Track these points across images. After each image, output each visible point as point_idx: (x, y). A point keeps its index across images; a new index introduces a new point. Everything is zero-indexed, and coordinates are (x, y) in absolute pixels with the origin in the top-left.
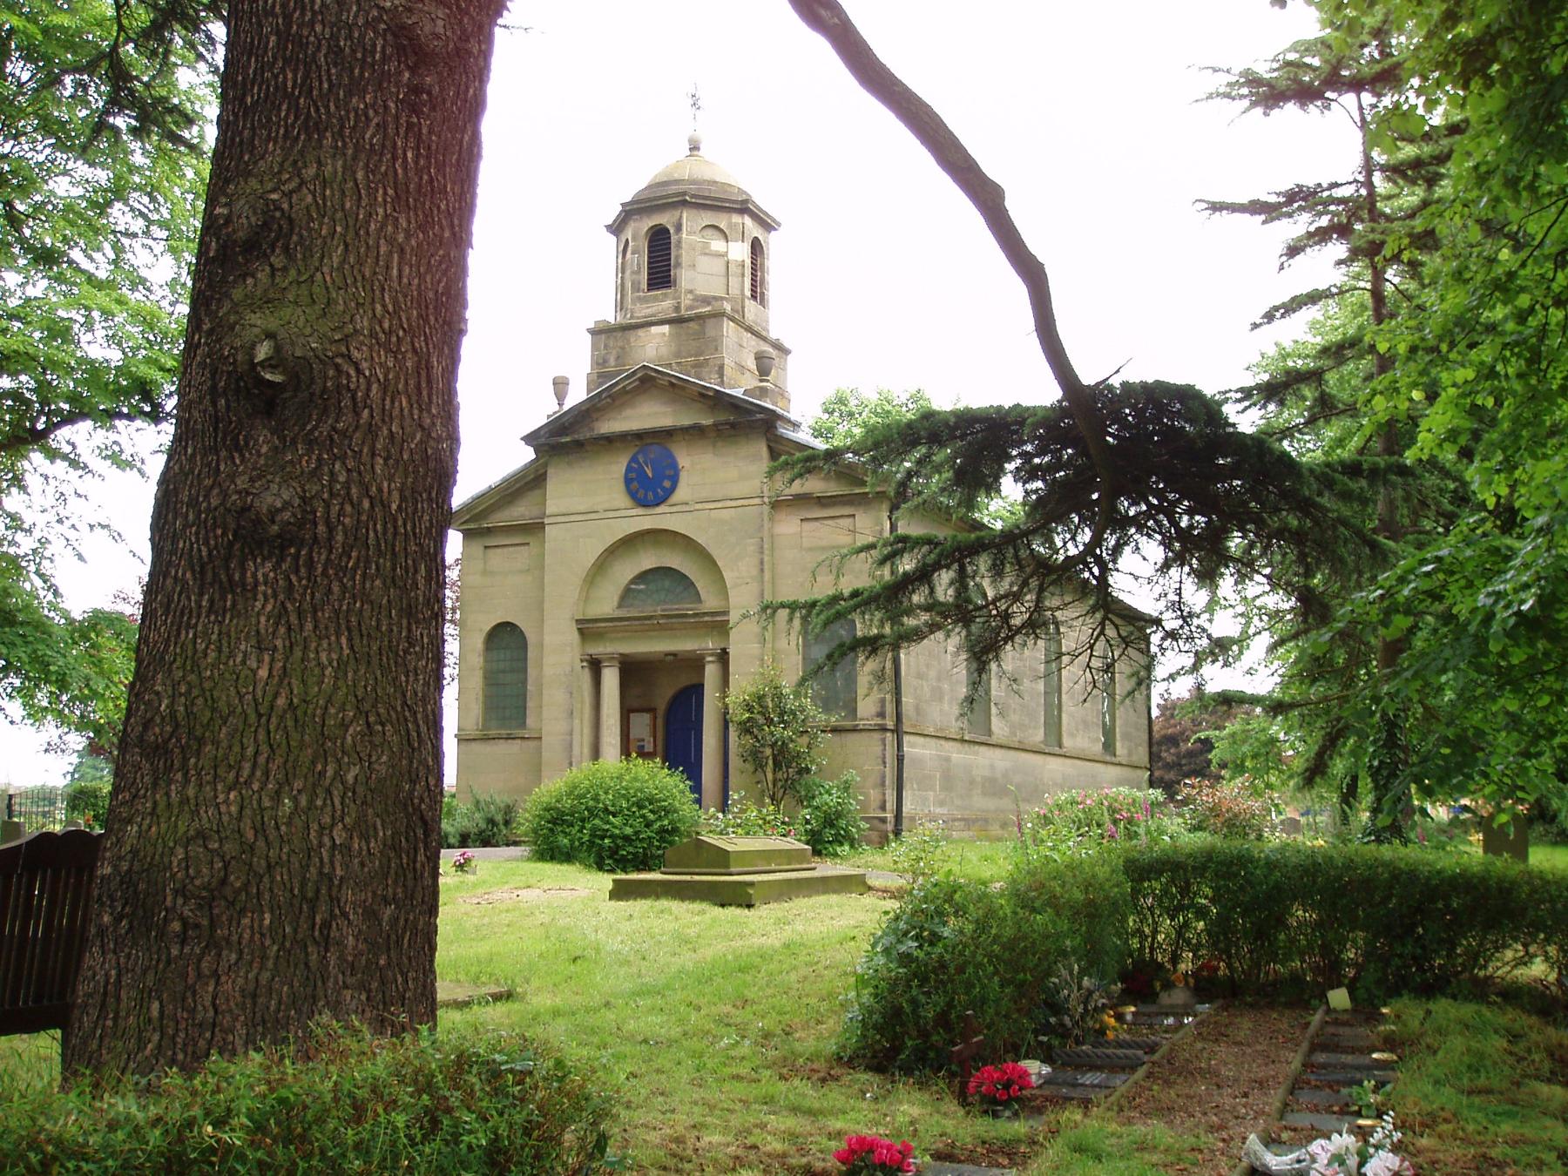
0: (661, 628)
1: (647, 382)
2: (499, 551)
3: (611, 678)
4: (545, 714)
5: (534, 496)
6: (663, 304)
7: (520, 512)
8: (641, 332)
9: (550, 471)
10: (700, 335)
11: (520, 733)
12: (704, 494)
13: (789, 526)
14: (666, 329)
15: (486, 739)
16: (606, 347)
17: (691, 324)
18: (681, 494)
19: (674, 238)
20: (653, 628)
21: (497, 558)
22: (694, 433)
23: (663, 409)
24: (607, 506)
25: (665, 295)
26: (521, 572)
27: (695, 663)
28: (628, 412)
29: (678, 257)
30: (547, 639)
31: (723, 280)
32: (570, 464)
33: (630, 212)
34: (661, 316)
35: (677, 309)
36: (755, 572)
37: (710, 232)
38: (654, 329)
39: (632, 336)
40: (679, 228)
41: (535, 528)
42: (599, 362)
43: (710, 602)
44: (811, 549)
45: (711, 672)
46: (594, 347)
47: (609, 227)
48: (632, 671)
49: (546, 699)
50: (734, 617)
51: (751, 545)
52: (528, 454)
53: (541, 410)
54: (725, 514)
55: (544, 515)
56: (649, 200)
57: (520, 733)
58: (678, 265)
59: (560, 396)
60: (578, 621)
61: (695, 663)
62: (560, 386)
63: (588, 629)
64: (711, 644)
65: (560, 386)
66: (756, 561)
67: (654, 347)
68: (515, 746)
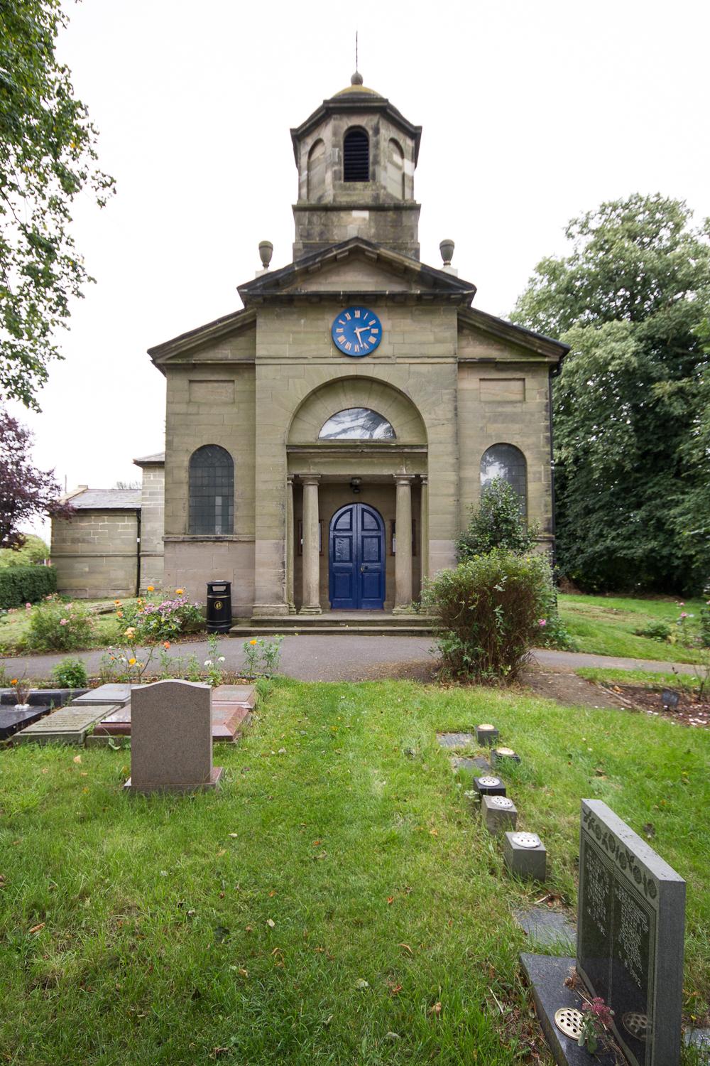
0: (362, 455)
1: (356, 253)
2: (204, 385)
3: (312, 494)
4: (258, 523)
5: (241, 341)
6: (362, 193)
7: (227, 353)
8: (343, 214)
9: (260, 321)
10: (397, 224)
11: (230, 537)
12: (406, 350)
13: (470, 382)
14: (366, 214)
15: (194, 541)
16: (310, 222)
17: (390, 214)
18: (384, 349)
19: (372, 140)
20: (355, 455)
21: (201, 391)
22: (398, 302)
23: (366, 279)
24: (315, 354)
25: (366, 187)
26: (226, 404)
27: (387, 487)
28: (334, 279)
29: (376, 156)
30: (259, 460)
31: (400, 188)
32: (278, 316)
33: (328, 111)
34: (362, 202)
35: (377, 197)
36: (450, 415)
37: (392, 146)
38: (356, 214)
39: (334, 216)
40: (377, 131)
41: (247, 367)
42: (303, 234)
43: (406, 437)
44: (489, 403)
45: (403, 492)
46: (298, 222)
47: (292, 131)
48: (327, 487)
49: (258, 510)
50: (432, 450)
51: (447, 395)
52: (236, 304)
53: (252, 270)
54: (424, 369)
55: (254, 357)
56: (353, 101)
57: (230, 537)
58: (376, 162)
59: (266, 259)
60: (288, 447)
61: (387, 487)
62: (266, 251)
63: (296, 454)
64: (405, 471)
65: (266, 251)
66: (450, 407)
67: (356, 224)
68: (223, 548)
